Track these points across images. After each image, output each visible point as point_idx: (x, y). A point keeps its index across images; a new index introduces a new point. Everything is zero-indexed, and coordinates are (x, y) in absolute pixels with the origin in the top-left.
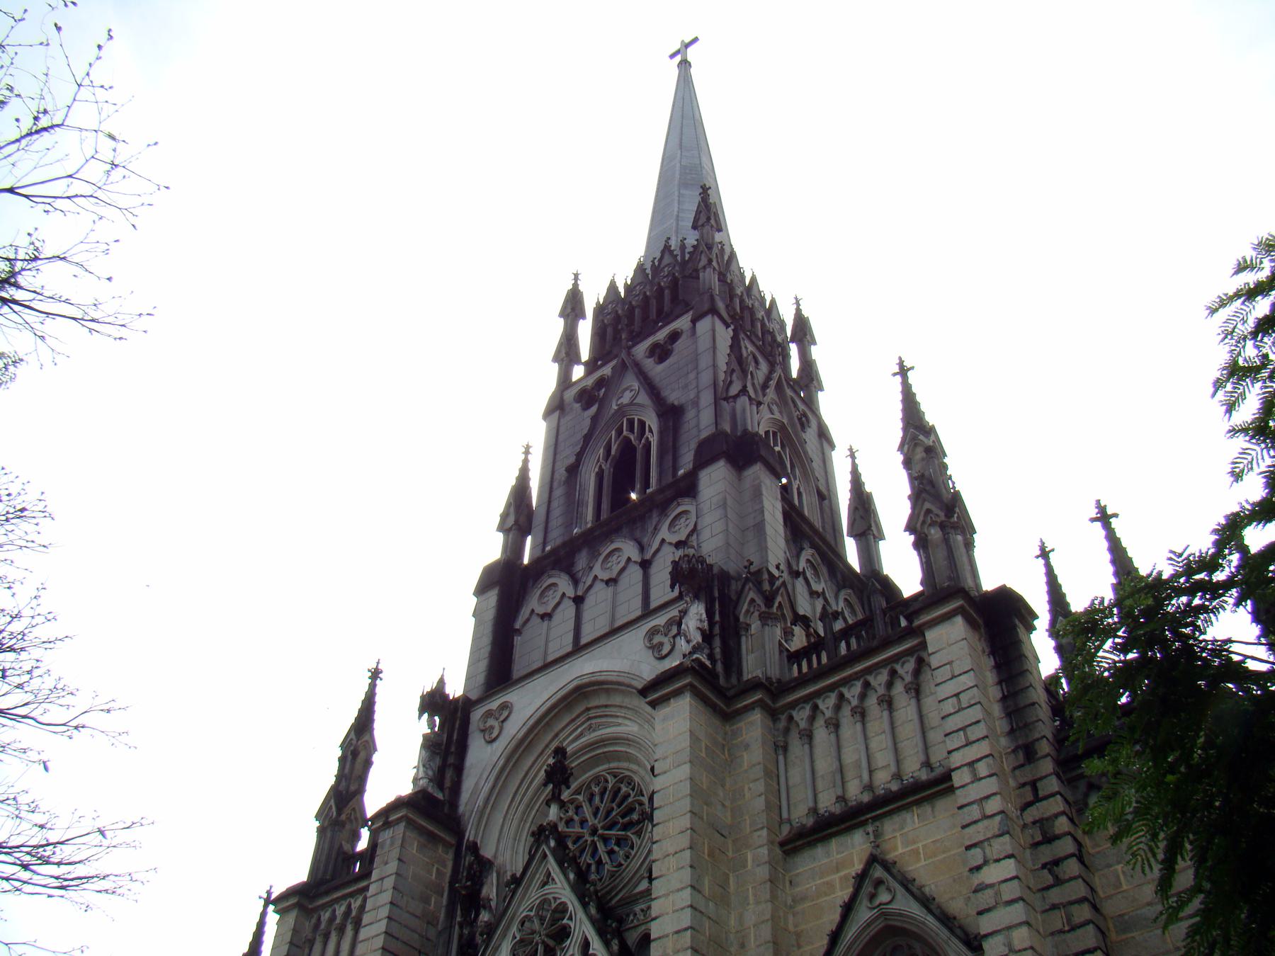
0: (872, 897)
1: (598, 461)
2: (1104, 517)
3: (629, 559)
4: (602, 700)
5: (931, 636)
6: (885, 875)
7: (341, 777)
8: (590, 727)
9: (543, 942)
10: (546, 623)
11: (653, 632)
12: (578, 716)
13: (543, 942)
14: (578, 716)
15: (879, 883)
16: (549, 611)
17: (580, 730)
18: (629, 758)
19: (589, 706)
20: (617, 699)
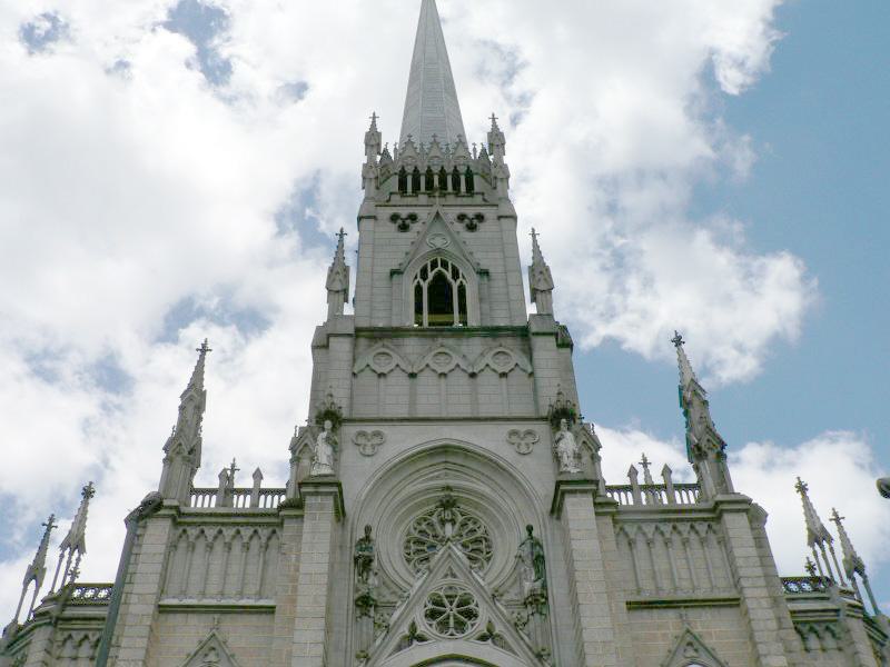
0: (685, 650)
1: (416, 277)
2: (802, 488)
3: (458, 366)
4: (459, 461)
5: (727, 517)
6: (694, 641)
7: (182, 420)
8: (446, 475)
9: (454, 615)
10: (382, 380)
11: (514, 433)
12: (439, 464)
13: (454, 615)
14: (439, 464)
15: (690, 644)
16: (385, 372)
17: (436, 474)
18: (477, 506)
19: (449, 460)
20: (474, 465)
